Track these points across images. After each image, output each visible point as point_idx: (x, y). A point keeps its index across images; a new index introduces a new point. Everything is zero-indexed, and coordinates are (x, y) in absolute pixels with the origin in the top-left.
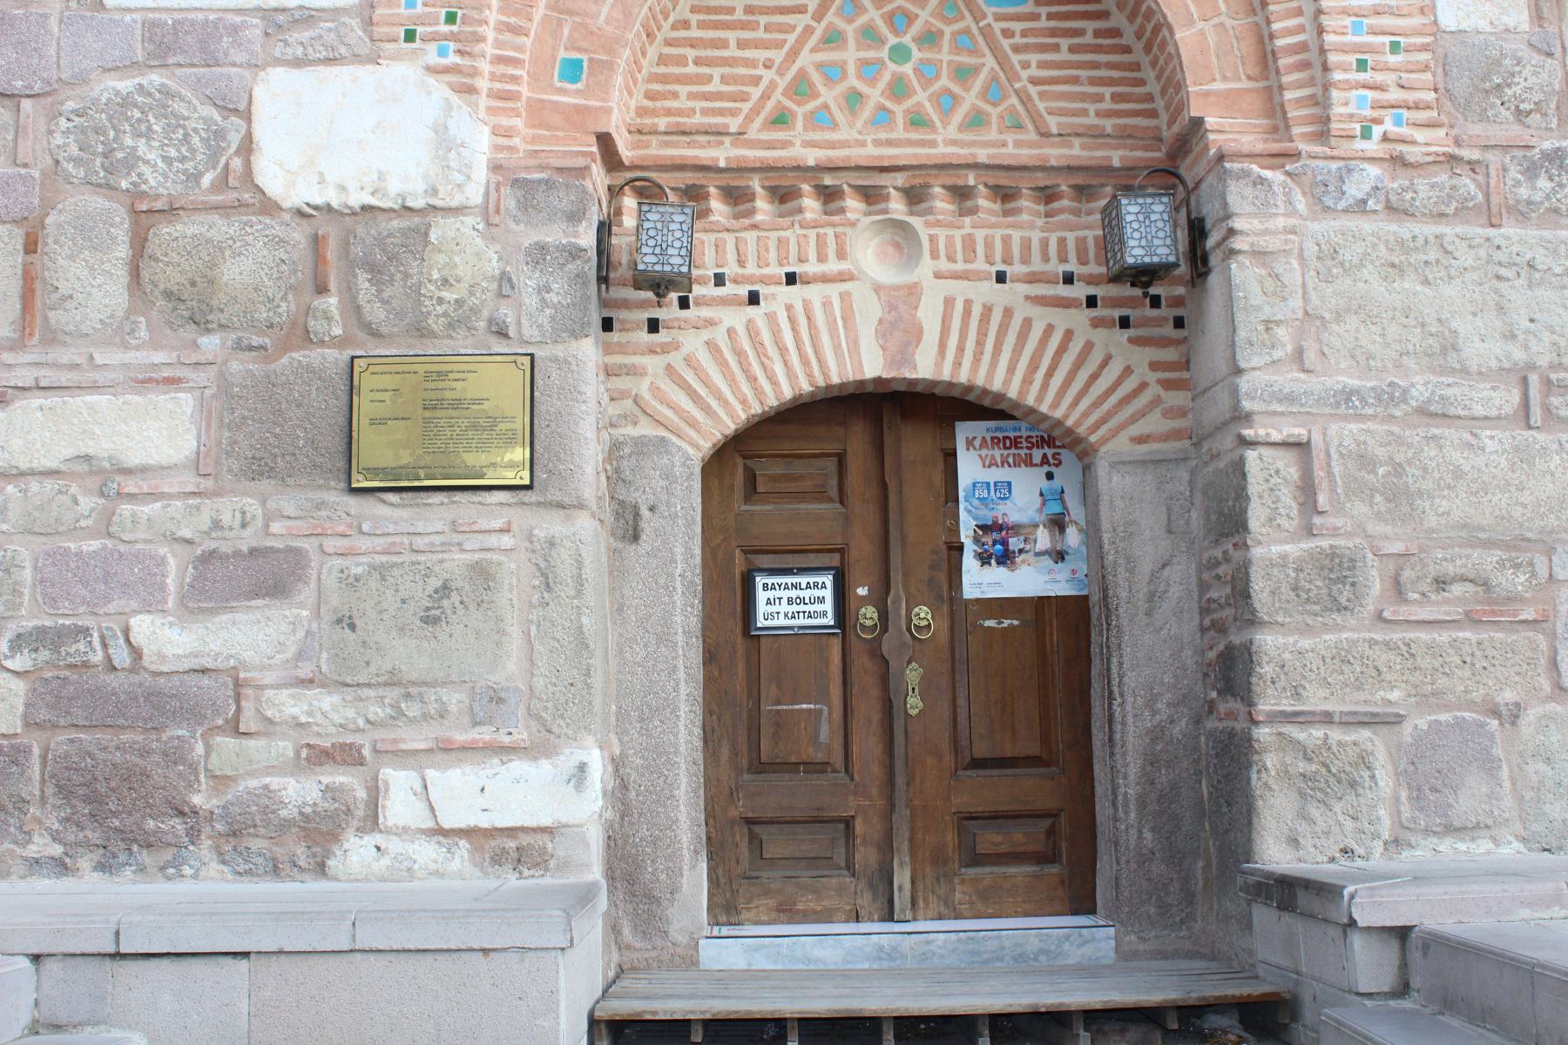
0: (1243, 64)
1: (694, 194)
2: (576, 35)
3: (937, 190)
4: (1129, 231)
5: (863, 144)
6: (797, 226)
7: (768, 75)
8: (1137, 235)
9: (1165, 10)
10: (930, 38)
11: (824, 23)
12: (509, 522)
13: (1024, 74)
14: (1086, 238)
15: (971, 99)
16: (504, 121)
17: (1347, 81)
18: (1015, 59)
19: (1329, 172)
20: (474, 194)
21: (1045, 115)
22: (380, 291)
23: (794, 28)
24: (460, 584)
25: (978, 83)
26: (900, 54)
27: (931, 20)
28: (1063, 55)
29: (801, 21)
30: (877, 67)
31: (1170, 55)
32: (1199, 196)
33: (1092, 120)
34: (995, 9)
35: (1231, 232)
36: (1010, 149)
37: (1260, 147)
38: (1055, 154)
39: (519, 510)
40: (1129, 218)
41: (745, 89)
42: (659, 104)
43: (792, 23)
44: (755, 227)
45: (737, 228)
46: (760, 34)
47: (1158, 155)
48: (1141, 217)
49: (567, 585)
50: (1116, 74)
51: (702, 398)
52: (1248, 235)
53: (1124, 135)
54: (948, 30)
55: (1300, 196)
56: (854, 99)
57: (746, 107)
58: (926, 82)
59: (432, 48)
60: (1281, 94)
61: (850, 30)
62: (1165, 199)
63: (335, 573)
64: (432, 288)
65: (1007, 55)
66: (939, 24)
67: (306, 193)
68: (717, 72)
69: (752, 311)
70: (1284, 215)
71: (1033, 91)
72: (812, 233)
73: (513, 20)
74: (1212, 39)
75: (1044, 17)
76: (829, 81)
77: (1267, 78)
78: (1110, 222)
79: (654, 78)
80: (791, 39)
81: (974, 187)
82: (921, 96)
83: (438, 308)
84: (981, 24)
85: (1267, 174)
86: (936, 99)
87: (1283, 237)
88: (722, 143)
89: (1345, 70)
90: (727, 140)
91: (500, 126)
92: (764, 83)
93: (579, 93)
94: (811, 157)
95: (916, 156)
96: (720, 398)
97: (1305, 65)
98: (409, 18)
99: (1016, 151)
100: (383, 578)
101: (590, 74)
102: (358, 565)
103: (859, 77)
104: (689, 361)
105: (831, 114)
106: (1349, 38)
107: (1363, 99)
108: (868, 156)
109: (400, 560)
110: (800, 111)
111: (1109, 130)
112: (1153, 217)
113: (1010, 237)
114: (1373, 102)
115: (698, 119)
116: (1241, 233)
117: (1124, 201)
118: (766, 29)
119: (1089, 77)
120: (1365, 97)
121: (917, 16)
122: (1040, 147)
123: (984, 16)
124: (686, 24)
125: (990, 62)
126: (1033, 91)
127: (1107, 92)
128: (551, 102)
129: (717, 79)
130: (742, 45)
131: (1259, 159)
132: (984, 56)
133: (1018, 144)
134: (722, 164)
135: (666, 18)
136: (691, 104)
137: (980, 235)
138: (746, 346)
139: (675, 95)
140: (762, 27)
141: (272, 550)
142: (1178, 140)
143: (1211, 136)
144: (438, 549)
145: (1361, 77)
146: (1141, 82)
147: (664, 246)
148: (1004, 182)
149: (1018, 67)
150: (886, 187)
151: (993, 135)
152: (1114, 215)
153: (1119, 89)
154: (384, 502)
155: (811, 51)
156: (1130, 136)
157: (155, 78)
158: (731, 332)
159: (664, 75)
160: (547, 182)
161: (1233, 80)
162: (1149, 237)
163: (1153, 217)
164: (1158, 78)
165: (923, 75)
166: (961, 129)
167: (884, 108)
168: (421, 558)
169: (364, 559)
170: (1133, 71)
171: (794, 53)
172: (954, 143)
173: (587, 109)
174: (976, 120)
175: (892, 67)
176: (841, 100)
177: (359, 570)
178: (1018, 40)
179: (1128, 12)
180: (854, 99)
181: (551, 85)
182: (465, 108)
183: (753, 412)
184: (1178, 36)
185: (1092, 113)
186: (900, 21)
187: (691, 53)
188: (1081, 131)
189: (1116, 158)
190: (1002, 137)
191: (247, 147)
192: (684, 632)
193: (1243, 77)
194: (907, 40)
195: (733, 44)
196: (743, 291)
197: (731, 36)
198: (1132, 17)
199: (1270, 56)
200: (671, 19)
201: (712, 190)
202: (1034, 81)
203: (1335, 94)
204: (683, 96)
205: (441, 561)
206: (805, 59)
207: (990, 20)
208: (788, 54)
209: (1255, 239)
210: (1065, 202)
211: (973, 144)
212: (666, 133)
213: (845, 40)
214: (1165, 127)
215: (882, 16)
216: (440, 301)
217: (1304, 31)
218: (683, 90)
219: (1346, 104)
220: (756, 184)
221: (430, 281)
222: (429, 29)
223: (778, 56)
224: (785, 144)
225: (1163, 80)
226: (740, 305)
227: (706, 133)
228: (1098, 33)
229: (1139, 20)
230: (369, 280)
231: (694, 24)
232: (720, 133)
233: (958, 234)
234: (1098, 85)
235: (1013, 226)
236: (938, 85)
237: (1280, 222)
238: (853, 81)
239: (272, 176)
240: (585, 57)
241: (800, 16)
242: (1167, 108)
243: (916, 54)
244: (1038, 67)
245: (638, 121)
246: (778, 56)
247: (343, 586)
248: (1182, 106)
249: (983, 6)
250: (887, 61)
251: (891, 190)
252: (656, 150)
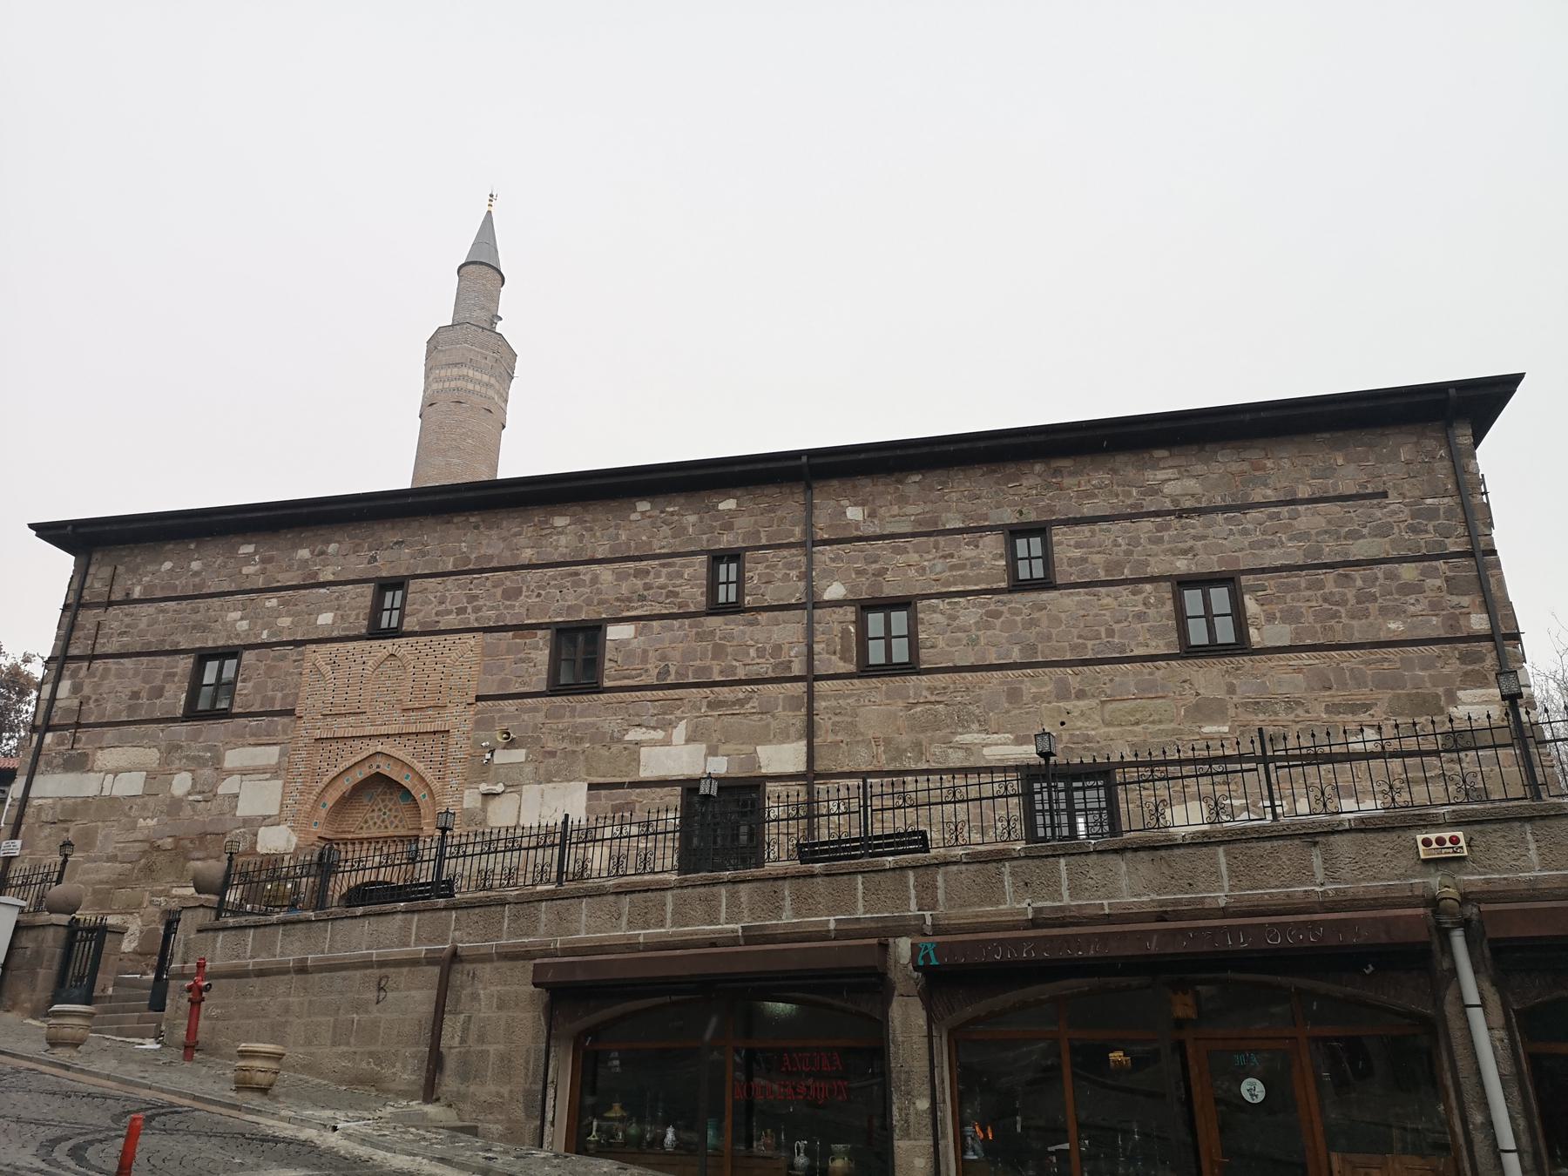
20: (292, 851)
26: (385, 814)
29: (368, 808)
56: (375, 823)
67: (265, 851)
94: (365, 836)
157: (242, 830)
174: (397, 827)
191: (256, 842)
239: (258, 849)
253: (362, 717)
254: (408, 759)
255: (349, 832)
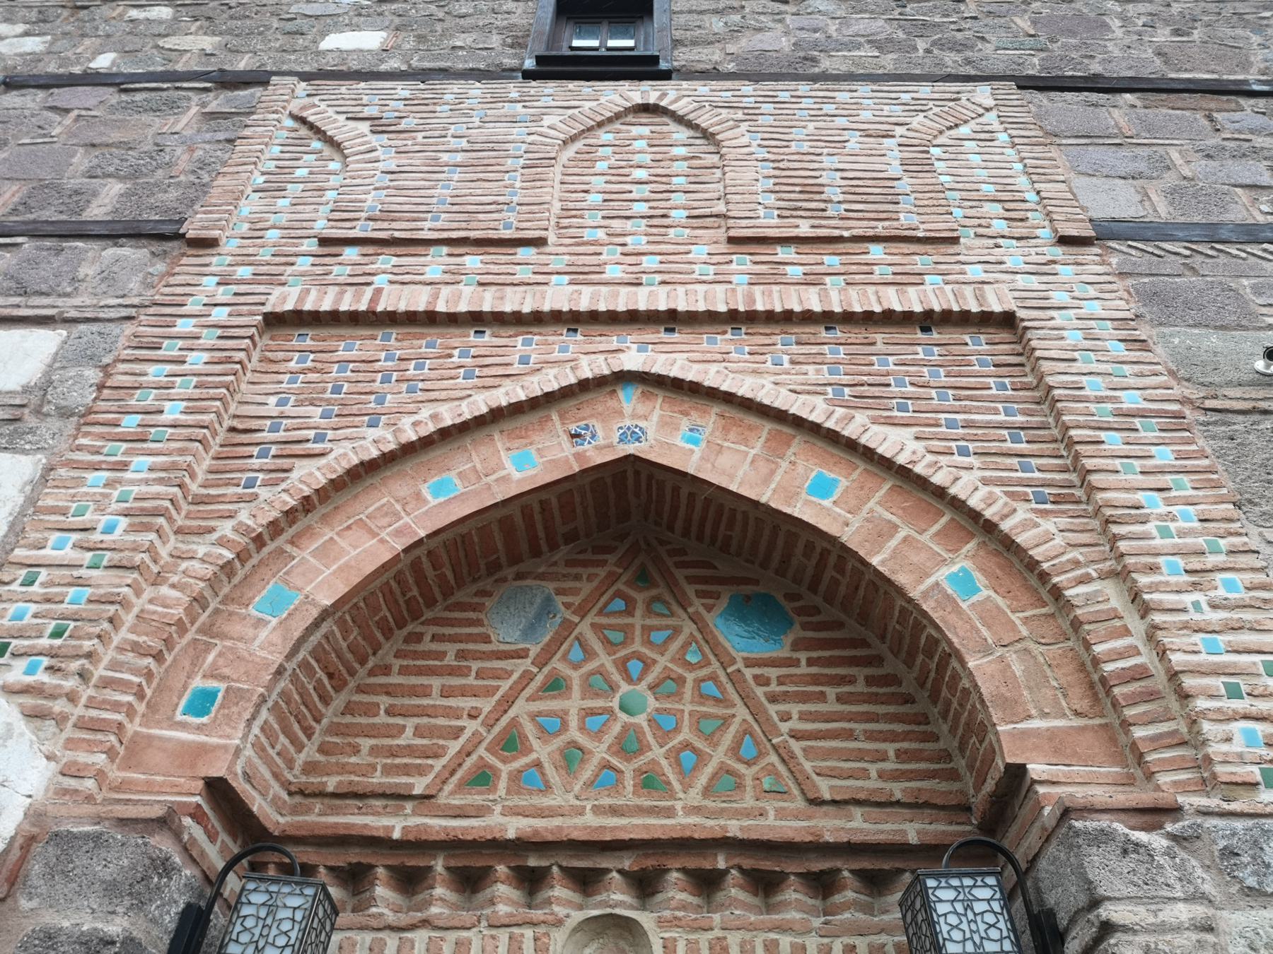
0: (1065, 696)
1: (355, 878)
2: (221, 662)
3: (675, 875)
4: (945, 928)
5: (580, 812)
6: (484, 923)
7: (472, 726)
8: (957, 935)
9: (950, 636)
10: (667, 686)
11: (546, 670)
13: (785, 727)
14: (884, 945)
15: (719, 756)
16: (83, 757)
17: (1219, 710)
18: (773, 709)
19: (1234, 834)
21: (814, 776)
23: (510, 674)
25: (728, 738)
27: (670, 665)
28: (831, 706)
29: (519, 667)
30: (605, 717)
31: (966, 692)
32: (1037, 880)
33: (873, 783)
34: (745, 655)
35: (1107, 928)
36: (771, 820)
37: (1123, 797)
38: (832, 827)
40: (942, 908)
41: (441, 742)
42: (333, 759)
43: (509, 668)
44: (425, 923)
45: (403, 924)
46: (471, 680)
47: (968, 828)
48: (959, 908)
50: (899, 728)
52: (1135, 932)
53: (917, 805)
54: (690, 677)
55: (1199, 872)
56: (571, 757)
57: (438, 764)
58: (664, 736)
59: (22, 664)
60: (1127, 733)
61: (575, 677)
62: (991, 881)
65: (761, 704)
66: (680, 671)
68: (410, 723)
70: (1185, 900)
71: (796, 746)
72: (503, 935)
73: (142, 639)
74: (1017, 668)
75: (803, 662)
76: (544, 733)
77: (1102, 716)
78: (914, 917)
79: (334, 729)
80: (505, 685)
81: (725, 873)
82: (657, 753)
84: (729, 670)
85: (1141, 836)
86: (675, 756)
87: (1194, 936)
88: (404, 808)
89: (1212, 697)
90: (409, 806)
91: (75, 763)
92: (467, 734)
93: (199, 728)
94: (513, 828)
95: (646, 827)
97: (1151, 696)
98: (9, 629)
99: (778, 823)
101: (222, 706)
103: (582, 728)
105: (543, 774)
106: (1202, 657)
107: (1249, 735)
108: (585, 828)
110: (505, 769)
111: (898, 795)
112: (979, 907)
113: (776, 943)
114: (1265, 737)
115: (377, 779)
116: (1125, 929)
117: (931, 883)
118: (478, 676)
119: (865, 731)
120: (1254, 731)
121: (655, 662)
122: (809, 818)
123: (733, 661)
124: (386, 670)
125: (742, 713)
126: (796, 746)
127: (891, 748)
128: (160, 738)
129: (409, 731)
130: (446, 693)
131: (1123, 816)
132: (734, 705)
133: (781, 815)
134: (396, 835)
135: (363, 662)
136: (371, 760)
137: (734, 939)
139: (356, 750)
140: (473, 674)
142: (993, 804)
143: (1041, 790)
145: (1237, 705)
146: (935, 738)
148: (767, 865)
149: (776, 718)
150: (608, 871)
151: (749, 801)
152: (918, 906)
153: (905, 745)
155: (528, 700)
156: (927, 805)
159: (347, 726)
160: (96, 838)
161: (1055, 718)
162: (977, 940)
163: (979, 907)
164: (953, 730)
165: (660, 727)
166: (707, 791)
167: (608, 766)
170: (920, 724)
171: (507, 702)
172: (697, 810)
173: (202, 750)
175: (623, 717)
176: (557, 757)
178: (774, 687)
179: (903, 655)
180: (571, 757)
181: (170, 718)
182: (29, 735)
184: (971, 665)
185: (874, 774)
186: (635, 667)
187: (384, 701)
188: (862, 796)
189: (912, 831)
190: (760, 804)
193: (1068, 712)
194: (642, 686)
195: (436, 691)
197: (436, 683)
198: (909, 663)
199: (1099, 687)
200: (370, 664)
201: (381, 871)
202: (796, 735)
203: (1206, 726)
204: (365, 750)
206: (520, 708)
207: (740, 665)
208: (499, 703)
209: (1151, 939)
210: (850, 895)
211: (720, 813)
212: (334, 795)
213: (569, 688)
214: (972, 791)
215: (615, 662)
217: (1139, 653)
218: (366, 743)
219: (1228, 740)
220: (439, 865)
222: (26, 643)
223: (486, 705)
224: (480, 812)
225: (960, 731)
227: (384, 796)
228: (870, 681)
229: (921, 657)
231: (396, 669)
232: (400, 796)
233: (704, 939)
234: (876, 740)
235: (782, 928)
236: (680, 738)
237: (1182, 912)
238: (574, 733)
240: (222, 686)
241: (519, 661)
242: (970, 767)
243: (652, 703)
244: (800, 719)
245: (303, 779)
246: (486, 705)
248: (992, 752)
249: (734, 653)
250: (617, 710)
251: (614, 874)
252: (321, 818)
253: (524, 253)
254: (815, 410)
255: (400, 796)
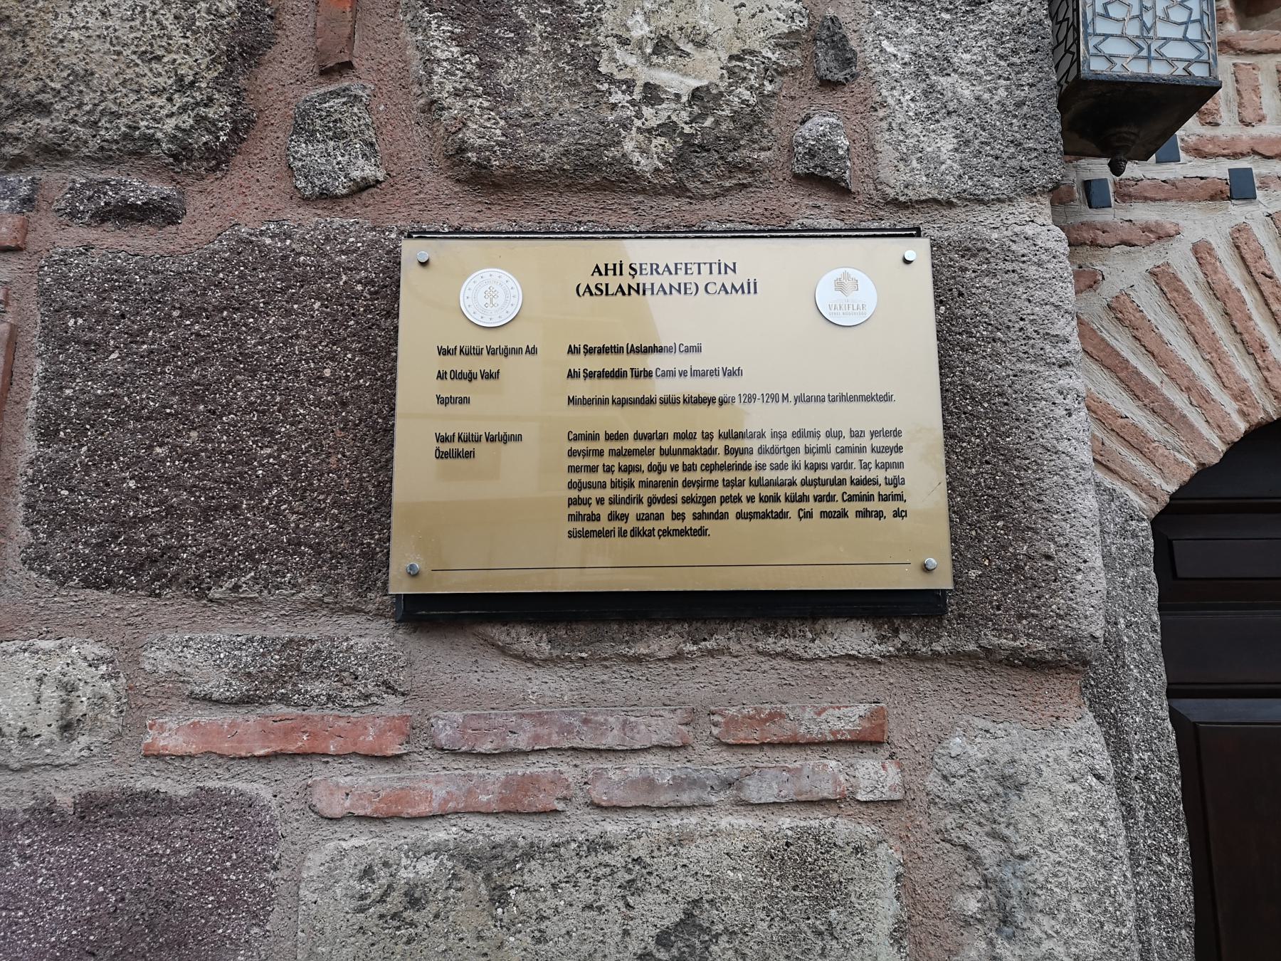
12: (878, 716)
22: (488, 67)
24: (730, 915)
39: (896, 675)
49: (1071, 921)
51: (1153, 388)
63: (347, 884)
64: (632, 61)
69: (1237, 212)
83: (647, 111)
96: (1190, 387)
100: (499, 897)
102: (417, 852)
104: (1117, 310)
109: (549, 837)
138: (1233, 274)
141: (155, 804)
144: (665, 798)
147: (1148, 18)
154: (503, 651)
158: (1201, 252)
168: (614, 827)
169: (440, 834)
177: (426, 867)
183: (1259, 416)
192: (1159, 915)
196: (1219, 170)
205: (681, 840)
216: (652, 94)
221: (624, 42)
226: (1212, 198)
230: (458, 40)
247: (371, 923)
